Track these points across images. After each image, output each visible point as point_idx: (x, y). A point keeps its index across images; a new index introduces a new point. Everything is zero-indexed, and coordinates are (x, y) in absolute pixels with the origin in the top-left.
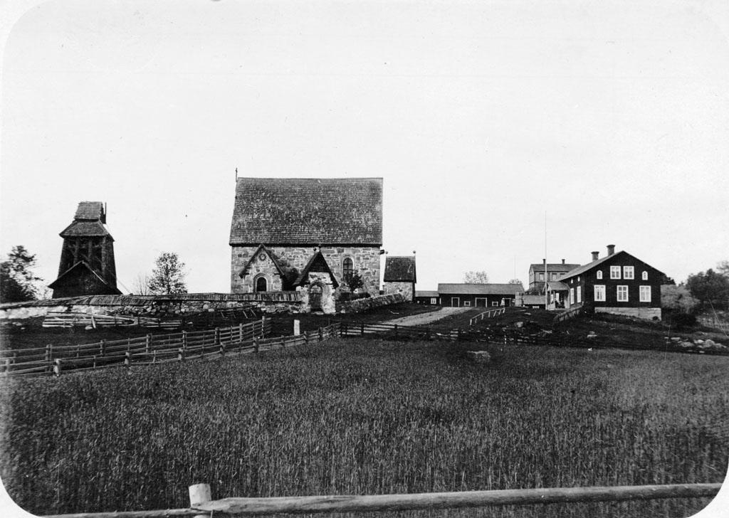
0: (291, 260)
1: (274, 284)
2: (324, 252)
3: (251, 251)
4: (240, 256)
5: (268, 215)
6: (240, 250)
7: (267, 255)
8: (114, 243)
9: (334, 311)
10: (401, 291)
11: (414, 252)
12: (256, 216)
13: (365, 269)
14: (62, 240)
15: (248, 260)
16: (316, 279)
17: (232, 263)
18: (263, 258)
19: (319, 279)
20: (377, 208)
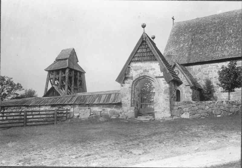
1: (186, 94)
7: (179, 71)
12: (182, 45)
16: (140, 71)
19: (145, 71)
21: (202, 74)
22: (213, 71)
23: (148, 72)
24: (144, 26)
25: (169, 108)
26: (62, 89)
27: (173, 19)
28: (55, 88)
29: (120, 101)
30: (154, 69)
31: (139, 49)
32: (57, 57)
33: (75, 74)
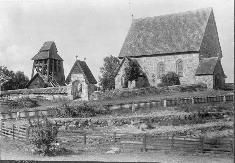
0: (149, 65)
2: (127, 60)
8: (63, 61)
10: (206, 81)
12: (136, 40)
13: (190, 68)
16: (75, 78)
19: (78, 78)
21: (146, 64)
22: (153, 62)
23: (79, 78)
24: (77, 57)
25: (87, 95)
26: (44, 75)
27: (133, 16)
28: (39, 74)
29: (66, 92)
30: (81, 77)
31: (75, 67)
32: (40, 48)
33: (55, 62)
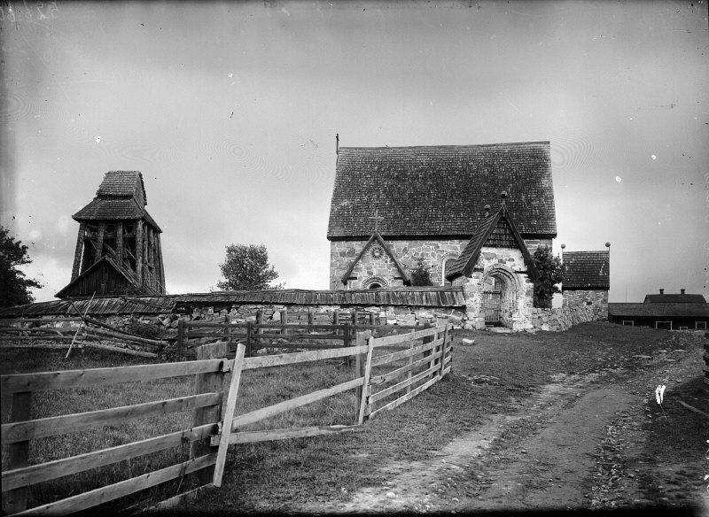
3: (358, 246)
4: (343, 254)
5: (383, 196)
6: (343, 246)
9: (529, 326)
10: (589, 304)
11: (608, 245)
14: (78, 225)
15: (353, 260)
16: (495, 261)
17: (332, 265)
18: (377, 254)
19: (501, 261)
20: (544, 182)
